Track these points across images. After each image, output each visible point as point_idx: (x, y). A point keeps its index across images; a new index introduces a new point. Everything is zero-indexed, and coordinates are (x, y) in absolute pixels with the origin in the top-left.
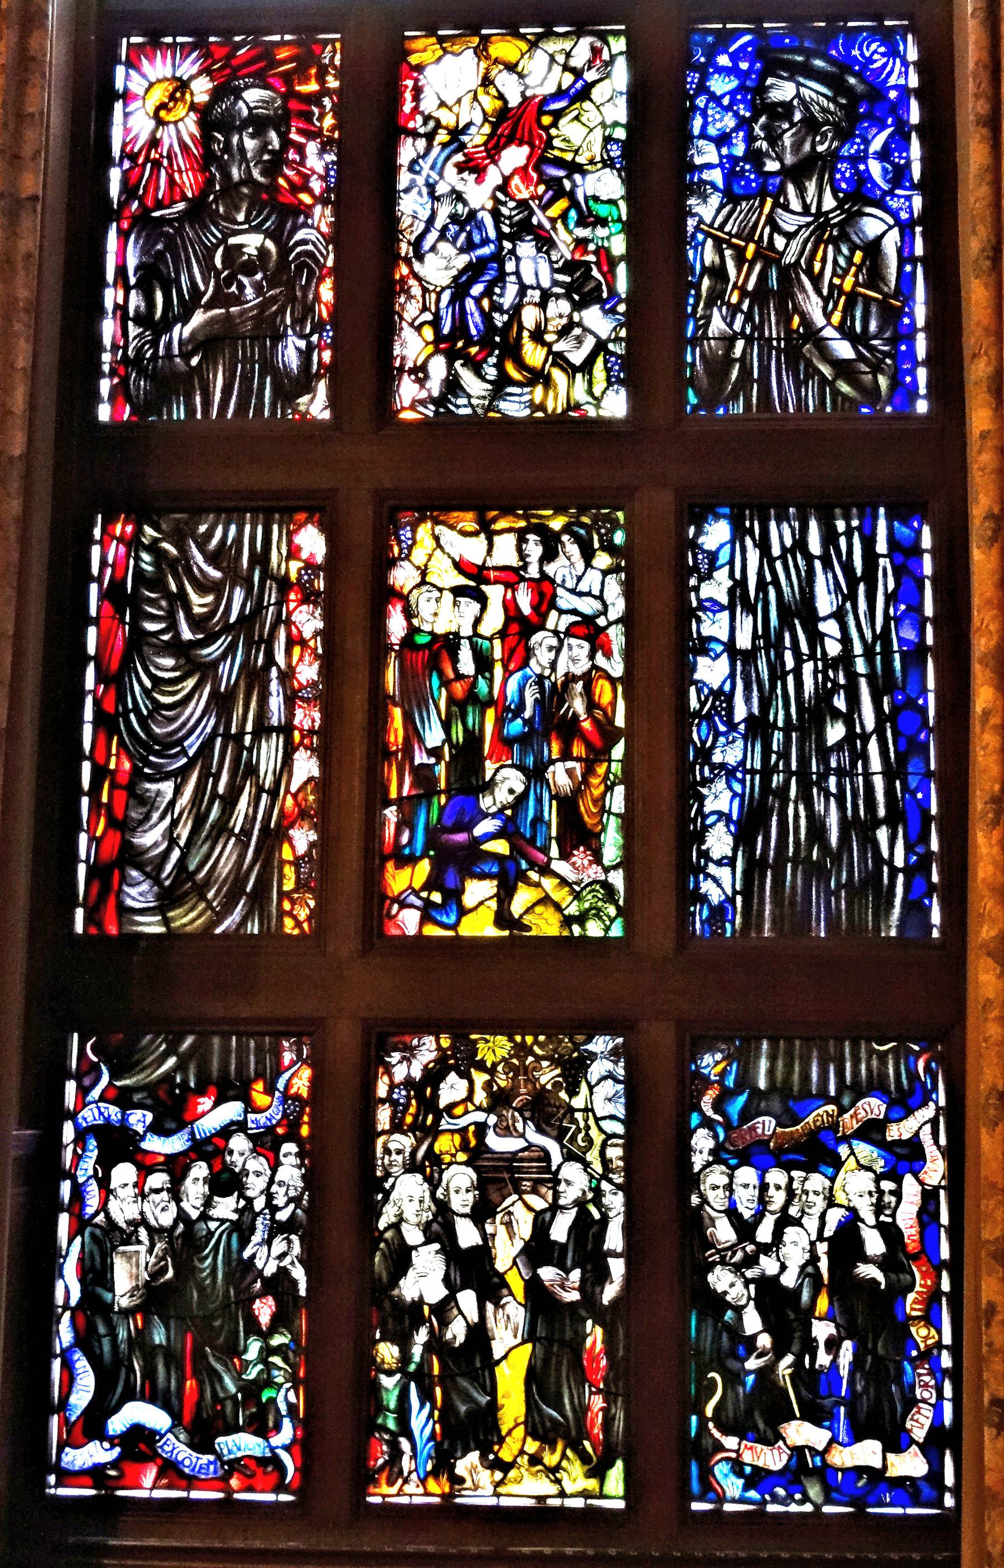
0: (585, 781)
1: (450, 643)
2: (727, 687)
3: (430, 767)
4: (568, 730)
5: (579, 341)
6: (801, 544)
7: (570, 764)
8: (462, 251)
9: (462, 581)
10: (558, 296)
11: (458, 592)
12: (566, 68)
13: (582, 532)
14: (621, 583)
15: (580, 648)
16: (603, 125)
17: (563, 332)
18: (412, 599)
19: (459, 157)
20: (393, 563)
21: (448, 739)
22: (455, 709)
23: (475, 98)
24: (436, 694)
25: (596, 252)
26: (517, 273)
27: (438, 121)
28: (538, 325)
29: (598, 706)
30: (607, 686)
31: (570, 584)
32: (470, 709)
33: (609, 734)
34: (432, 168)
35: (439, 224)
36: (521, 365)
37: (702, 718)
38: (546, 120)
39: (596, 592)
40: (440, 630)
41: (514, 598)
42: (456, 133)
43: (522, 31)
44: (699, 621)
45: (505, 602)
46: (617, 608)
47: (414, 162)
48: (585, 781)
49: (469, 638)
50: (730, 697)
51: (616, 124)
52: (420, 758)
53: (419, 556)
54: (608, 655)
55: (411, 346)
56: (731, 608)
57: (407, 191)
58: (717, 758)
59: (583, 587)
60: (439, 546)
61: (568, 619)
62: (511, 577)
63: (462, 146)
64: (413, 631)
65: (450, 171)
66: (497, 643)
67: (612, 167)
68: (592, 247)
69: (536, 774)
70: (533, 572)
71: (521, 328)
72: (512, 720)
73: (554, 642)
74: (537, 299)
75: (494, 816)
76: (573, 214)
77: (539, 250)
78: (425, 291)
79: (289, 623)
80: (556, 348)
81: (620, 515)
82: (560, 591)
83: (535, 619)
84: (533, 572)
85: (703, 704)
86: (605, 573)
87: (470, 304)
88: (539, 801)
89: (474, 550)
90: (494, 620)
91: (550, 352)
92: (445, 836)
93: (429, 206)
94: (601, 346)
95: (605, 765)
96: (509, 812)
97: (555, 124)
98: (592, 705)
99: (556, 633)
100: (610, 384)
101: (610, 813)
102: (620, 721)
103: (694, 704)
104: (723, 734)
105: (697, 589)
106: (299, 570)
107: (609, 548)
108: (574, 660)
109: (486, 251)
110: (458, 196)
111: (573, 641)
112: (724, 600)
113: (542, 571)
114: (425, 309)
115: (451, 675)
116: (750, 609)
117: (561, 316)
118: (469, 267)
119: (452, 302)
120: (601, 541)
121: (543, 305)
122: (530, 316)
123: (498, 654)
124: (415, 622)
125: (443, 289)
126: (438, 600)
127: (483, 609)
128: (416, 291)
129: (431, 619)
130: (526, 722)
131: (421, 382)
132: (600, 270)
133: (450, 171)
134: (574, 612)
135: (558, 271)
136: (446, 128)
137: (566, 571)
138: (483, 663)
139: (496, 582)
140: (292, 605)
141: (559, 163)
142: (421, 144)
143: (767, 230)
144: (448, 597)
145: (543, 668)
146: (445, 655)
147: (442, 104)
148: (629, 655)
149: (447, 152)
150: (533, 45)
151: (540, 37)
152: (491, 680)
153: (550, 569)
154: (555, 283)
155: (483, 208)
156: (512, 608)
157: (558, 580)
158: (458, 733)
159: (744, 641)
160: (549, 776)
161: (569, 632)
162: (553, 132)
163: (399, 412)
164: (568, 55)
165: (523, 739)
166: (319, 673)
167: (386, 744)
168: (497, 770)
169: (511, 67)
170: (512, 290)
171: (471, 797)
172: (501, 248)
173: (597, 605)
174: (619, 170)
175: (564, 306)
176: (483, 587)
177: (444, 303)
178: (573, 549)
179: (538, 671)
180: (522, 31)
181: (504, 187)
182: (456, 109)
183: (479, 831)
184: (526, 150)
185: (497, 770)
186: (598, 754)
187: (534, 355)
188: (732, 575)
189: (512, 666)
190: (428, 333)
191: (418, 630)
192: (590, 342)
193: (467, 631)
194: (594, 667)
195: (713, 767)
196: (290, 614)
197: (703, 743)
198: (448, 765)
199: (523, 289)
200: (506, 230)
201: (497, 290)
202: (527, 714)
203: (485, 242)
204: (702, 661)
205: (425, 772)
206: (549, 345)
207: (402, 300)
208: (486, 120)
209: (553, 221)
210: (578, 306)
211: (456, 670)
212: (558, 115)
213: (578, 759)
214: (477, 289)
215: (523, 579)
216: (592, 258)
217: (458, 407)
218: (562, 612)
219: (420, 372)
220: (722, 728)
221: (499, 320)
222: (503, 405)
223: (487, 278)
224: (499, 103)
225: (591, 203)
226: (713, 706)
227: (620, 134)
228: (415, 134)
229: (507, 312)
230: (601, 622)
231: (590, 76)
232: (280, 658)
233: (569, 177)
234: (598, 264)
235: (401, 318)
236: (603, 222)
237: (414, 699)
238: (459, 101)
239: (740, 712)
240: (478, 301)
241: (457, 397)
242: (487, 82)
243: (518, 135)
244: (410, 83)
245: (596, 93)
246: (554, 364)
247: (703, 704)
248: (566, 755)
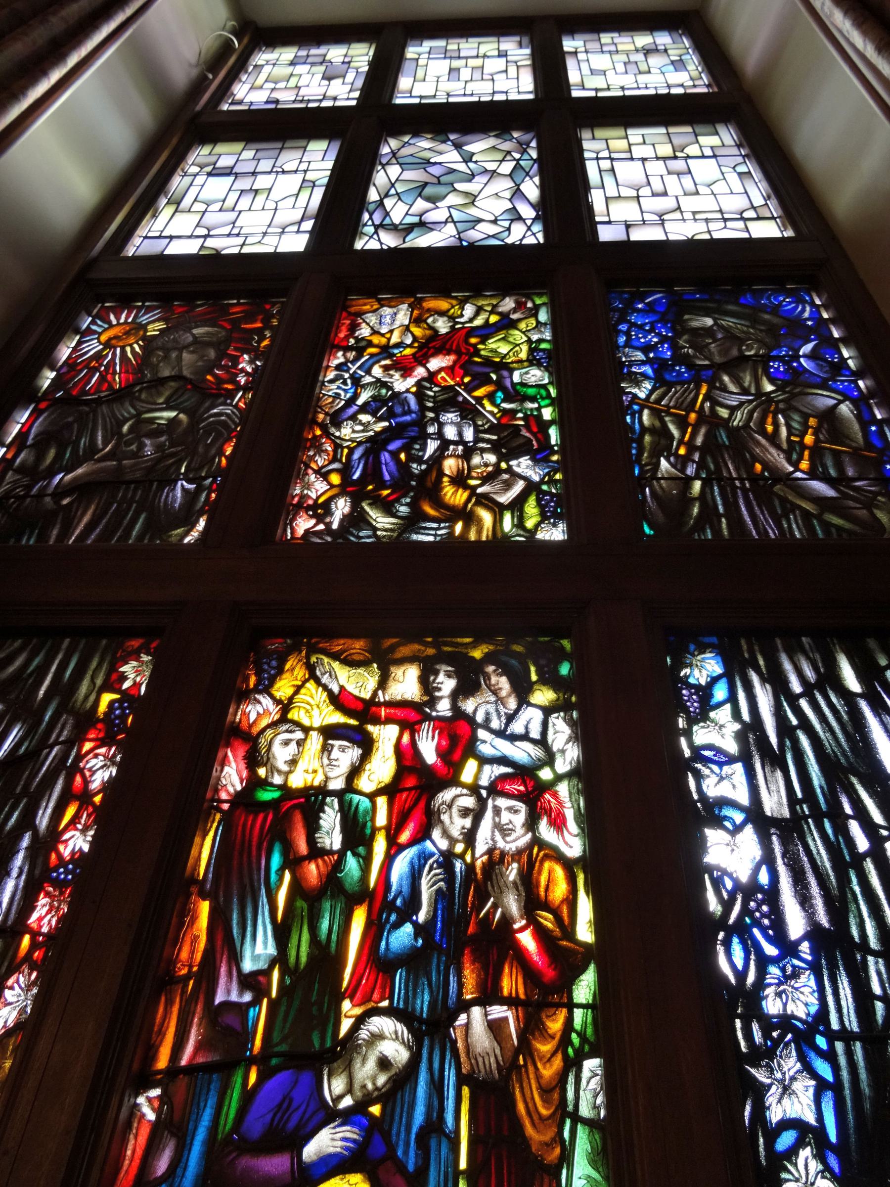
0: (525, 1046)
1: (311, 801)
2: (764, 878)
3: (242, 1009)
4: (497, 944)
5: (508, 485)
6: (829, 679)
7: (498, 1011)
9: (338, 718)
10: (483, 450)
11: (330, 732)
13: (514, 662)
14: (571, 723)
15: (514, 813)
17: (487, 479)
18: (263, 742)
20: (246, 696)
21: (280, 959)
22: (300, 904)
24: (273, 877)
29: (546, 906)
30: (559, 873)
31: (495, 724)
32: (327, 905)
33: (566, 959)
36: (438, 502)
37: (731, 931)
39: (535, 734)
40: (297, 781)
41: (413, 742)
44: (698, 776)
45: (398, 747)
46: (568, 756)
48: (525, 1046)
49: (339, 795)
50: (772, 894)
52: (228, 992)
53: (283, 688)
54: (558, 823)
56: (745, 758)
58: (772, 1006)
59: (517, 727)
60: (313, 676)
61: (491, 772)
62: (410, 716)
64: (254, 783)
66: (382, 802)
67: (539, 365)
69: (431, 1030)
70: (444, 708)
71: (441, 474)
72: (397, 925)
73: (469, 802)
75: (346, 1117)
79: (75, 769)
81: (566, 644)
82: (482, 734)
83: (443, 771)
84: (444, 708)
85: (728, 906)
86: (547, 711)
87: (385, 457)
88: (437, 1087)
89: (360, 683)
90: (381, 768)
92: (246, 1162)
95: (562, 1014)
96: (376, 1110)
98: (533, 902)
99: (474, 789)
101: (576, 1118)
102: (585, 933)
103: (714, 906)
104: (774, 961)
105: (688, 733)
106: (111, 703)
107: (550, 679)
108: (504, 830)
111: (502, 802)
112: (732, 747)
113: (455, 707)
114: (334, 459)
115: (303, 847)
116: (775, 760)
119: (365, 455)
120: (538, 673)
122: (450, 465)
123: (381, 819)
124: (262, 772)
126: (300, 743)
127: (366, 756)
128: (329, 447)
129: (285, 768)
130: (419, 930)
133: (377, 371)
134: (503, 760)
137: (491, 708)
138: (356, 834)
139: (389, 720)
140: (88, 746)
143: (708, 404)
144: (315, 741)
145: (453, 841)
146: (298, 818)
148: (591, 824)
152: (366, 861)
153: (469, 705)
154: (477, 440)
156: (409, 754)
157: (480, 718)
158: (301, 948)
159: (774, 803)
160: (457, 1034)
161: (495, 789)
165: (413, 961)
166: (92, 844)
167: (172, 962)
168: (360, 1021)
171: (306, 1077)
173: (536, 752)
174: (544, 367)
176: (370, 728)
178: (504, 684)
179: (443, 844)
183: (311, 1151)
185: (360, 1021)
186: (545, 994)
188: (736, 714)
189: (404, 837)
190: (335, 479)
191: (265, 783)
192: (520, 486)
193: (337, 784)
194: (537, 841)
195: (767, 1023)
196: (80, 757)
197: (741, 975)
198: (273, 1006)
202: (422, 917)
204: (713, 836)
205: (230, 1019)
206: (473, 489)
207: (311, 453)
209: (479, 400)
210: (506, 458)
211: (311, 841)
213: (511, 1002)
215: (428, 718)
216: (522, 423)
218: (484, 761)
219: (321, 510)
220: (771, 950)
224: (428, 332)
225: (518, 387)
226: (745, 911)
228: (347, 349)
229: (426, 462)
230: (545, 774)
232: (43, 821)
234: (527, 427)
237: (236, 884)
239: (796, 924)
240: (395, 455)
243: (448, 346)
247: (728, 906)
248: (489, 994)
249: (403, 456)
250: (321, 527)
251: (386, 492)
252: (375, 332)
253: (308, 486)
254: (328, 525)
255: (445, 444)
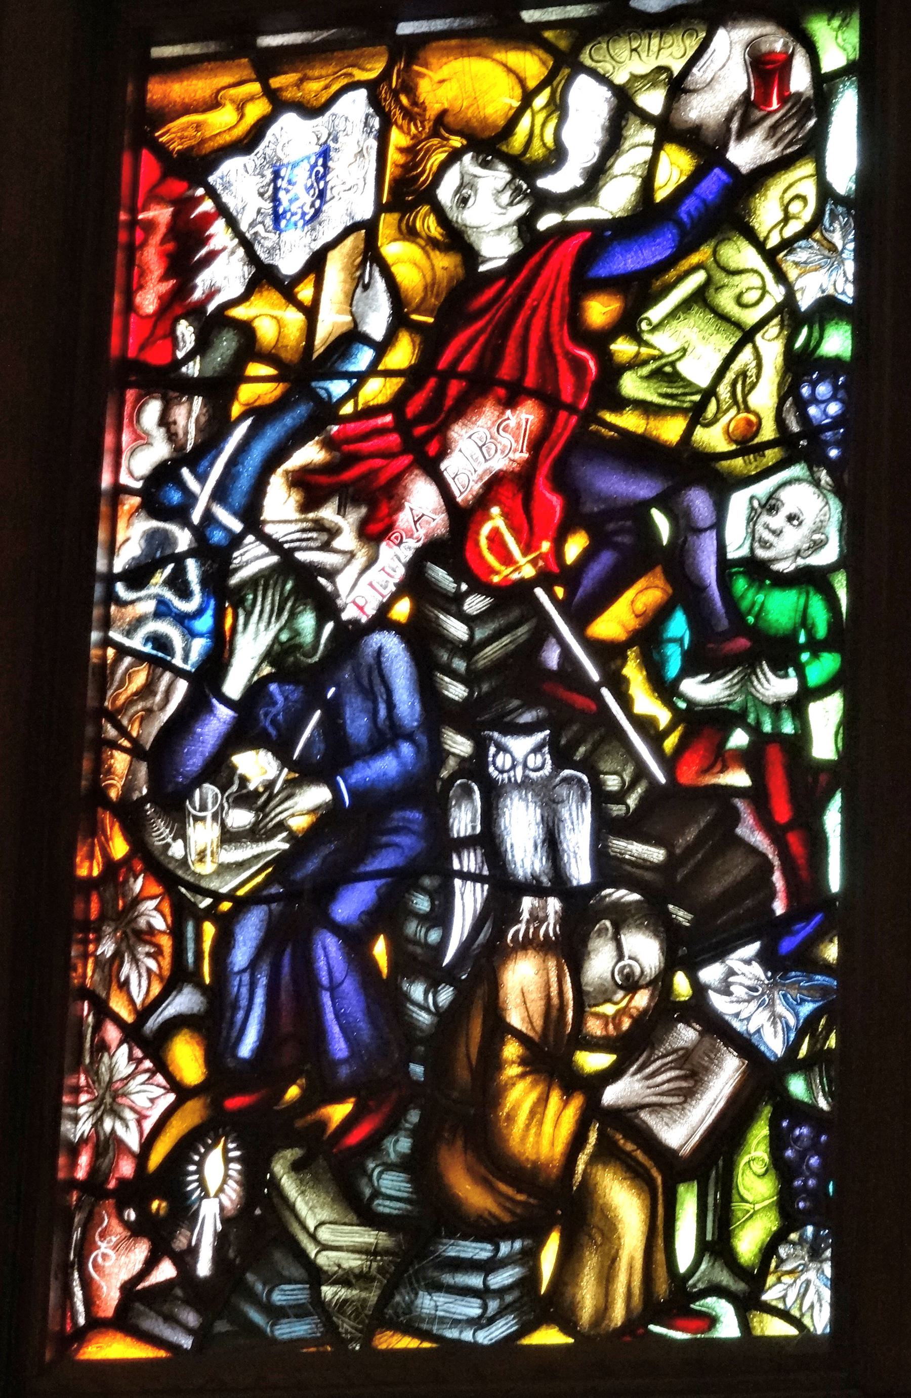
5: (693, 1074)
8: (305, 772)
10: (621, 917)
12: (669, 130)
16: (789, 314)
17: (634, 1045)
19: (311, 454)
23: (371, 253)
25: (749, 759)
26: (489, 840)
27: (246, 329)
28: (552, 1014)
34: (220, 494)
35: (235, 685)
38: (599, 311)
42: (304, 371)
43: (529, 16)
47: (164, 474)
51: (829, 309)
55: (133, 1104)
57: (137, 576)
63: (327, 411)
65: (280, 505)
67: (813, 457)
68: (739, 739)
71: (498, 1028)
74: (550, 927)
76: (678, 625)
77: (562, 757)
78: (182, 913)
80: (613, 1095)
87: (329, 952)
91: (594, 1111)
93: (205, 623)
94: (763, 1079)
97: (628, 324)
100: (789, 1217)
109: (386, 766)
110: (304, 585)
114: (179, 976)
117: (630, 985)
118: (327, 819)
121: (570, 949)
122: (524, 982)
125: (242, 905)
128: (154, 916)
131: (161, 1237)
132: (766, 823)
133: (280, 505)
135: (630, 827)
136: (269, 358)
141: (640, 452)
142: (189, 415)
147: (263, 277)
149: (272, 435)
150: (565, 64)
151: (586, 33)
154: (608, 868)
155: (381, 620)
162: (623, 348)
163: (82, 1336)
164: (678, 87)
169: (488, 143)
170: (468, 900)
172: (437, 753)
174: (833, 468)
175: (645, 950)
177: (241, 956)
180: (529, 16)
181: (451, 548)
182: (305, 292)
184: (526, 416)
187: (538, 1124)
190: (188, 1059)
192: (726, 1074)
199: (504, 890)
200: (456, 691)
201: (422, 903)
203: (387, 736)
207: (107, 948)
208: (400, 320)
209: (609, 654)
210: (687, 950)
212: (640, 291)
214: (350, 905)
216: (739, 778)
217: (276, 1313)
219: (157, 1199)
221: (424, 1000)
222: (429, 1303)
223: (386, 860)
224: (445, 262)
225: (740, 584)
227: (837, 342)
228: (169, 384)
229: (449, 976)
231: (746, 153)
233: (665, 502)
235: (103, 1012)
236: (781, 652)
238: (316, 264)
240: (356, 941)
241: (276, 1280)
242: (406, 193)
243: (506, 371)
244: (162, 214)
245: (766, 213)
246: (607, 1153)
249: (380, 950)
250: (166, 1271)
251: (339, 1112)
252: (263, 277)
253: (110, 1101)
254: (185, 1260)
255: (504, 890)
